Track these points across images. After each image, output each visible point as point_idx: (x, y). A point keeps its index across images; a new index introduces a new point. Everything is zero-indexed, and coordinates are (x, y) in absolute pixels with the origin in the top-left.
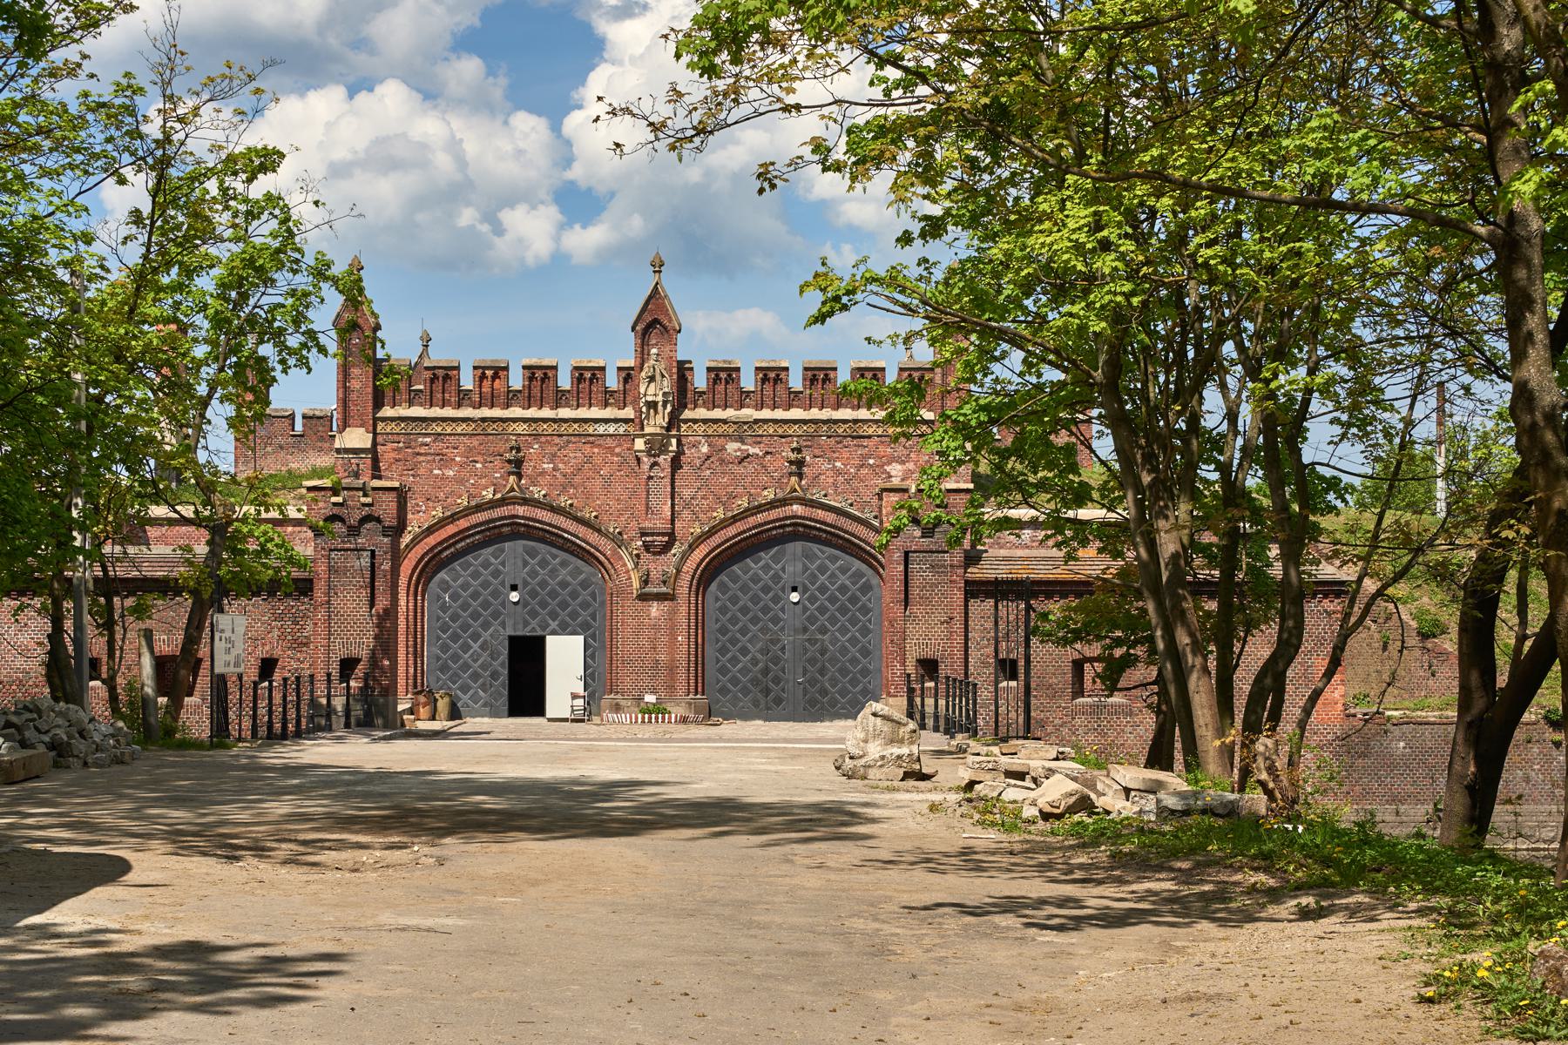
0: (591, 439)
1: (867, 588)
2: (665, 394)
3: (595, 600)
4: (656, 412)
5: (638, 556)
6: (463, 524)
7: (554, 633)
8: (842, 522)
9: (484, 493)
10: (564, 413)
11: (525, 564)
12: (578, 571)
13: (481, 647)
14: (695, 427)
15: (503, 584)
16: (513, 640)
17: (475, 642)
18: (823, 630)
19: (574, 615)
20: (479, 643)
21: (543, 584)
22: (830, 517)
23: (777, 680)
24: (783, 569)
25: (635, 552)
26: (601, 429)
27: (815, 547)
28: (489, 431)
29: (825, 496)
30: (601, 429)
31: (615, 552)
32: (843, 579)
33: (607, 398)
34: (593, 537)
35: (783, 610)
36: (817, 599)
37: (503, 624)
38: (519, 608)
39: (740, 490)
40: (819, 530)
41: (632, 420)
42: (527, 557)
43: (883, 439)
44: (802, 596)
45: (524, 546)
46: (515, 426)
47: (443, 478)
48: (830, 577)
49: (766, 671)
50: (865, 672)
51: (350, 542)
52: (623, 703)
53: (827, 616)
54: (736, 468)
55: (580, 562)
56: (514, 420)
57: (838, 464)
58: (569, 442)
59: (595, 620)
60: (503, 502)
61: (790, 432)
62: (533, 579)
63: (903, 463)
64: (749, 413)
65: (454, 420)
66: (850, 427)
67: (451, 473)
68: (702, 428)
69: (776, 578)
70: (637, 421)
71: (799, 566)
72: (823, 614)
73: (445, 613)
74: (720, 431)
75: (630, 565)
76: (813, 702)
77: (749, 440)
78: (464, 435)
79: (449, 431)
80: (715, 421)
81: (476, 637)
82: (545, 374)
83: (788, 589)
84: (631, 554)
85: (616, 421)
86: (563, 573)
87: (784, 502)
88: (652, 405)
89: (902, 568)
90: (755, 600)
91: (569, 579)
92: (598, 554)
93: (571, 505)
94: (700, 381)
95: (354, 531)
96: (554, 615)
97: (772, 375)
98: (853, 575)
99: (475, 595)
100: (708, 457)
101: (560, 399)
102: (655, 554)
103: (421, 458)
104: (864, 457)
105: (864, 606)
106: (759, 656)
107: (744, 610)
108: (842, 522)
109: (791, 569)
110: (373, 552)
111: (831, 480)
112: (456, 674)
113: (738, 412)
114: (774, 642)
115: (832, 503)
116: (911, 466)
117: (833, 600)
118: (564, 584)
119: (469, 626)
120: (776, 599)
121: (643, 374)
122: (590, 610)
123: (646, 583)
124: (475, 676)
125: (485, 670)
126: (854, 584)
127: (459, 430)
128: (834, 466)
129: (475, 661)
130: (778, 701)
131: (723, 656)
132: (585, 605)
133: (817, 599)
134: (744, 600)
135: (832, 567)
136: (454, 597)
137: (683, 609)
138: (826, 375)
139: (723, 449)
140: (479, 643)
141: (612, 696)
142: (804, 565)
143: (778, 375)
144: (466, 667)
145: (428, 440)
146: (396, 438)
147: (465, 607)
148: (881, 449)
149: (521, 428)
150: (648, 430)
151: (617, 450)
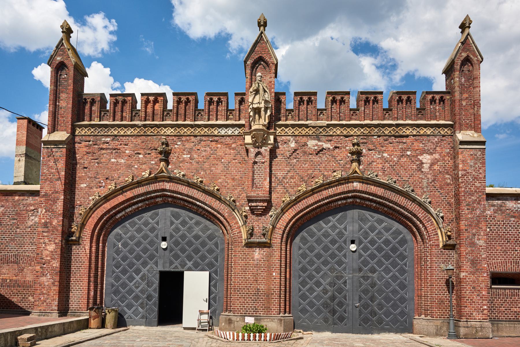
0: (216, 138)
1: (403, 242)
7: (189, 269)
8: (389, 194)
9: (143, 173)
12: (207, 228)
13: (141, 278)
14: (286, 130)
15: (157, 236)
16: (163, 275)
17: (137, 275)
19: (203, 258)
20: (140, 276)
21: (183, 237)
22: (380, 191)
23: (340, 304)
28: (148, 133)
29: (377, 176)
30: (223, 132)
31: (230, 215)
32: (387, 235)
34: (216, 204)
35: (345, 256)
38: (167, 252)
43: (417, 138)
45: (172, 212)
48: (377, 234)
49: (333, 298)
50: (403, 300)
52: (234, 318)
53: (375, 260)
54: (316, 159)
55: (208, 223)
57: (385, 155)
59: (217, 261)
60: (155, 179)
61: (352, 133)
63: (431, 154)
67: (123, 161)
69: (341, 234)
71: (356, 226)
72: (372, 259)
73: (118, 255)
74: (304, 133)
75: (241, 223)
76: (366, 320)
77: (324, 139)
81: (137, 272)
83: (349, 242)
86: (197, 230)
87: (346, 180)
88: (257, 111)
91: (200, 233)
92: (219, 216)
99: (138, 244)
102: (257, 215)
105: (401, 254)
106: (328, 287)
107: (318, 256)
108: (389, 194)
109: (351, 228)
111: (381, 166)
112: (124, 296)
114: (339, 278)
116: (437, 156)
119: (134, 264)
122: (214, 255)
123: (251, 235)
125: (144, 294)
128: (383, 157)
130: (341, 319)
131: (304, 287)
132: (210, 251)
134: (318, 249)
135: (379, 227)
136: (125, 245)
137: (277, 254)
139: (305, 145)
140: (140, 276)
141: (227, 313)
142: (360, 225)
144: (130, 292)
145: (108, 139)
147: (131, 251)
148: (416, 144)
149: (169, 131)
151: (233, 146)
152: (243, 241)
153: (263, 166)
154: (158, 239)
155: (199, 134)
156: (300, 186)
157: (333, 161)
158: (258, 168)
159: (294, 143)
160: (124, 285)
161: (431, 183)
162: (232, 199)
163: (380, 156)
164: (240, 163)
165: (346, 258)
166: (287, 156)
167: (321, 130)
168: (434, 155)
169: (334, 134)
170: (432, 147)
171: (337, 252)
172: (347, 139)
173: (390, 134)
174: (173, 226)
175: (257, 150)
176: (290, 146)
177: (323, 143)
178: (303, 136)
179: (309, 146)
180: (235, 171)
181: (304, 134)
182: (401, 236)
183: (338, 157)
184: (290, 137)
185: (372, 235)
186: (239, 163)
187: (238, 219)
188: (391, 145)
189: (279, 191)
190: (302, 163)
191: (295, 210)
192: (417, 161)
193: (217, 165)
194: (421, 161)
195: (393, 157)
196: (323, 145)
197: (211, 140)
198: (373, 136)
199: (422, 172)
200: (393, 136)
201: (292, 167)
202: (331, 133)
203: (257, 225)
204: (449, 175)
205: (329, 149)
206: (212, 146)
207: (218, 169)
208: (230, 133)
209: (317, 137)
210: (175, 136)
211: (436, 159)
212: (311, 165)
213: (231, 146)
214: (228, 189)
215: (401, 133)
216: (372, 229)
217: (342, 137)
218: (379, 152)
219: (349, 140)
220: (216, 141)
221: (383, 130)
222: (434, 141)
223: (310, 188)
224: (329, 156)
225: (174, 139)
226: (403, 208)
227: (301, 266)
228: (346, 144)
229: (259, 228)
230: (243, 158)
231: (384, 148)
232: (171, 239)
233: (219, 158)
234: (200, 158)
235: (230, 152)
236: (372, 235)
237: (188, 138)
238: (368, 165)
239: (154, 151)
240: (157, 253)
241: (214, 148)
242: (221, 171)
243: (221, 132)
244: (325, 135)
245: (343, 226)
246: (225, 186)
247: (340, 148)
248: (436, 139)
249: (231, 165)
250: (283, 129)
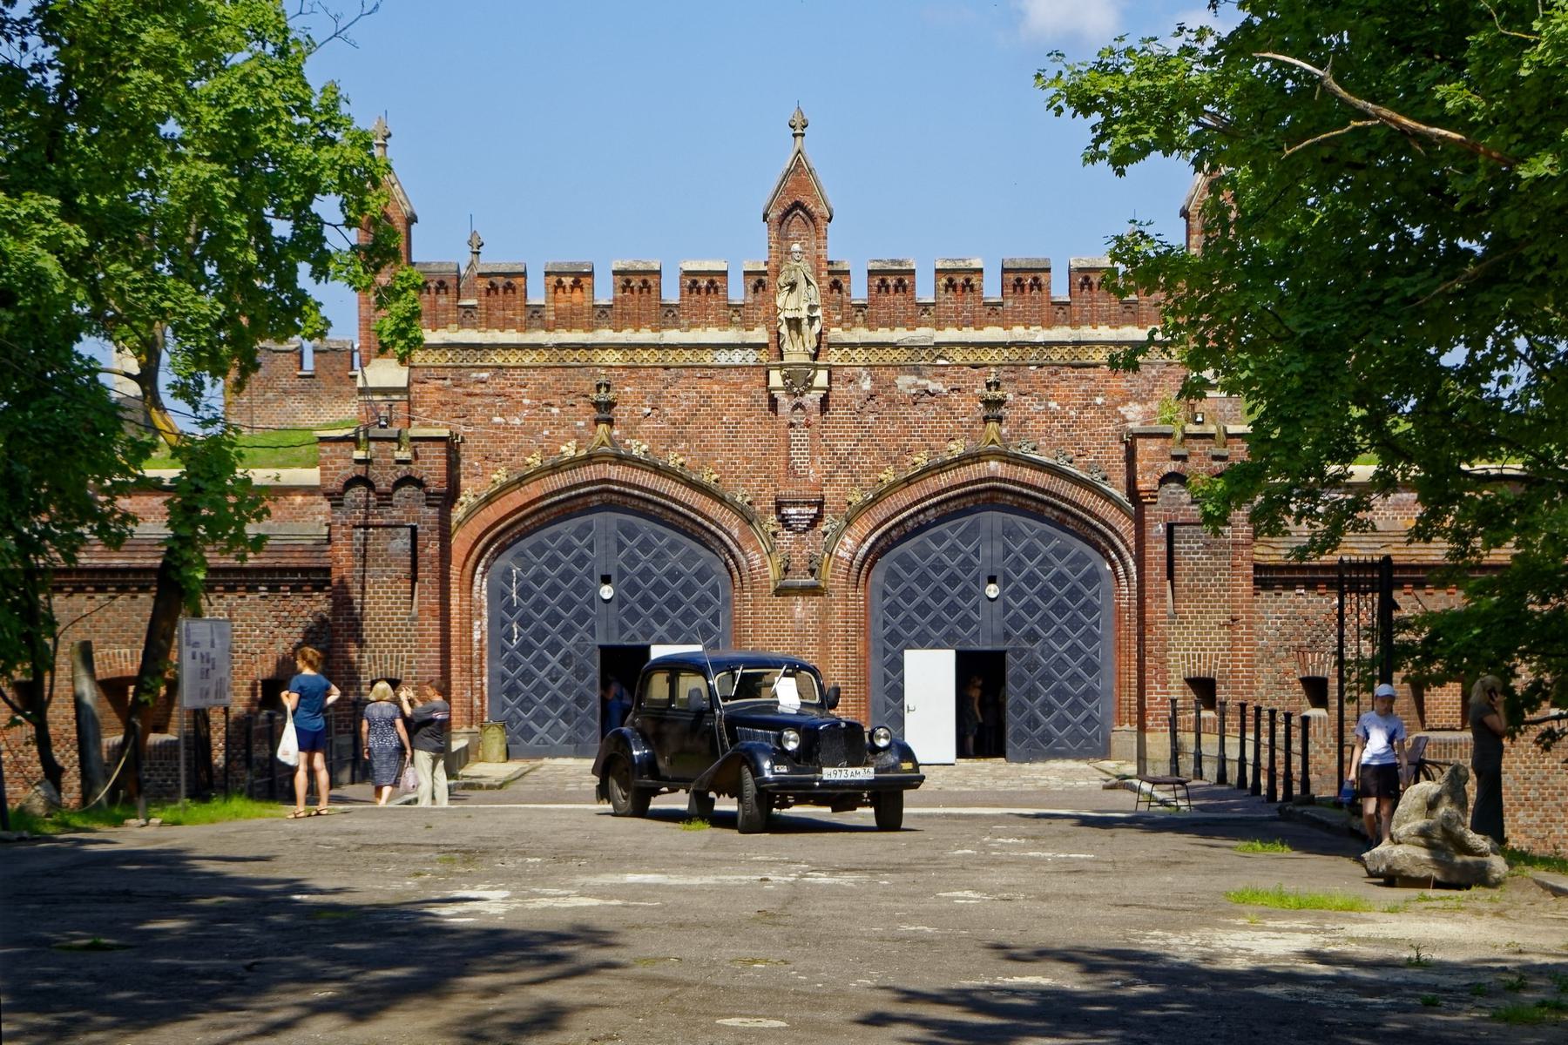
0: (709, 372)
2: (812, 308)
3: (717, 597)
4: (799, 332)
5: (774, 534)
6: (533, 490)
10: (672, 336)
11: (621, 546)
12: (690, 558)
13: (563, 661)
14: (853, 354)
15: (590, 574)
16: (607, 652)
17: (554, 654)
18: (1032, 636)
19: (688, 617)
20: (559, 656)
21: (646, 574)
22: (1041, 479)
24: (976, 553)
25: (772, 529)
26: (723, 358)
27: (1020, 521)
28: (569, 362)
30: (723, 358)
32: (1060, 566)
33: (737, 315)
34: (714, 510)
35: (976, 608)
36: (1023, 594)
37: (591, 630)
38: (613, 607)
39: (916, 442)
40: (1027, 496)
41: (766, 346)
42: (623, 538)
44: (1002, 590)
45: (619, 522)
46: (603, 354)
47: (507, 427)
48: (1041, 563)
50: (1090, 694)
51: (380, 514)
53: (1038, 616)
55: (694, 545)
56: (603, 347)
58: (679, 376)
59: (717, 624)
60: (589, 459)
61: (986, 360)
62: (632, 567)
63: (1144, 401)
64: (924, 334)
65: (520, 347)
66: (1070, 353)
67: (517, 421)
68: (860, 356)
69: (967, 564)
70: (773, 346)
71: (999, 549)
77: (929, 372)
78: (535, 368)
79: (513, 362)
80: (881, 345)
81: (554, 647)
82: (645, 282)
85: (743, 346)
86: (673, 560)
89: (1163, 548)
90: (938, 594)
91: (681, 567)
92: (720, 533)
93: (682, 465)
94: (859, 290)
95: (385, 499)
96: (660, 617)
97: (960, 280)
98: (1072, 561)
99: (553, 590)
101: (668, 315)
103: (476, 401)
104: (1090, 394)
107: (923, 609)
109: (988, 552)
110: (414, 529)
112: (528, 699)
113: (911, 333)
115: (1044, 459)
117: (1045, 594)
118: (673, 575)
119: (545, 633)
120: (966, 594)
121: (781, 280)
122: (711, 611)
123: (786, 570)
124: (554, 701)
125: (569, 694)
126: (1075, 572)
127: (527, 361)
128: (1048, 408)
129: (554, 680)
133: (1023, 594)
135: (1045, 549)
137: (839, 608)
138: (1036, 279)
140: (559, 656)
142: (1005, 545)
143: (968, 280)
144: (541, 689)
145: (485, 375)
146: (441, 373)
148: (1113, 382)
149: (613, 357)
150: (787, 359)
152: (772, 584)
154: (592, 579)
155: (674, 363)
156: (881, 470)
160: (527, 676)
163: (1042, 407)
165: (978, 613)
167: (923, 353)
168: (1150, 404)
170: (1146, 387)
171: (960, 602)
172: (976, 371)
173: (1062, 362)
174: (623, 554)
177: (929, 382)
178: (888, 366)
182: (1088, 566)
185: (1031, 565)
188: (1064, 383)
192: (1115, 417)
194: (1123, 416)
198: (1029, 365)
209: (917, 371)
210: (623, 367)
215: (1084, 360)
216: (1031, 552)
218: (1040, 400)
221: (1048, 352)
223: (903, 476)
226: (1088, 512)
227: (888, 629)
231: (1049, 392)
232: (620, 580)
236: (1031, 565)
238: (1019, 426)
239: (582, 399)
240: (593, 609)
245: (971, 548)
248: (1154, 372)
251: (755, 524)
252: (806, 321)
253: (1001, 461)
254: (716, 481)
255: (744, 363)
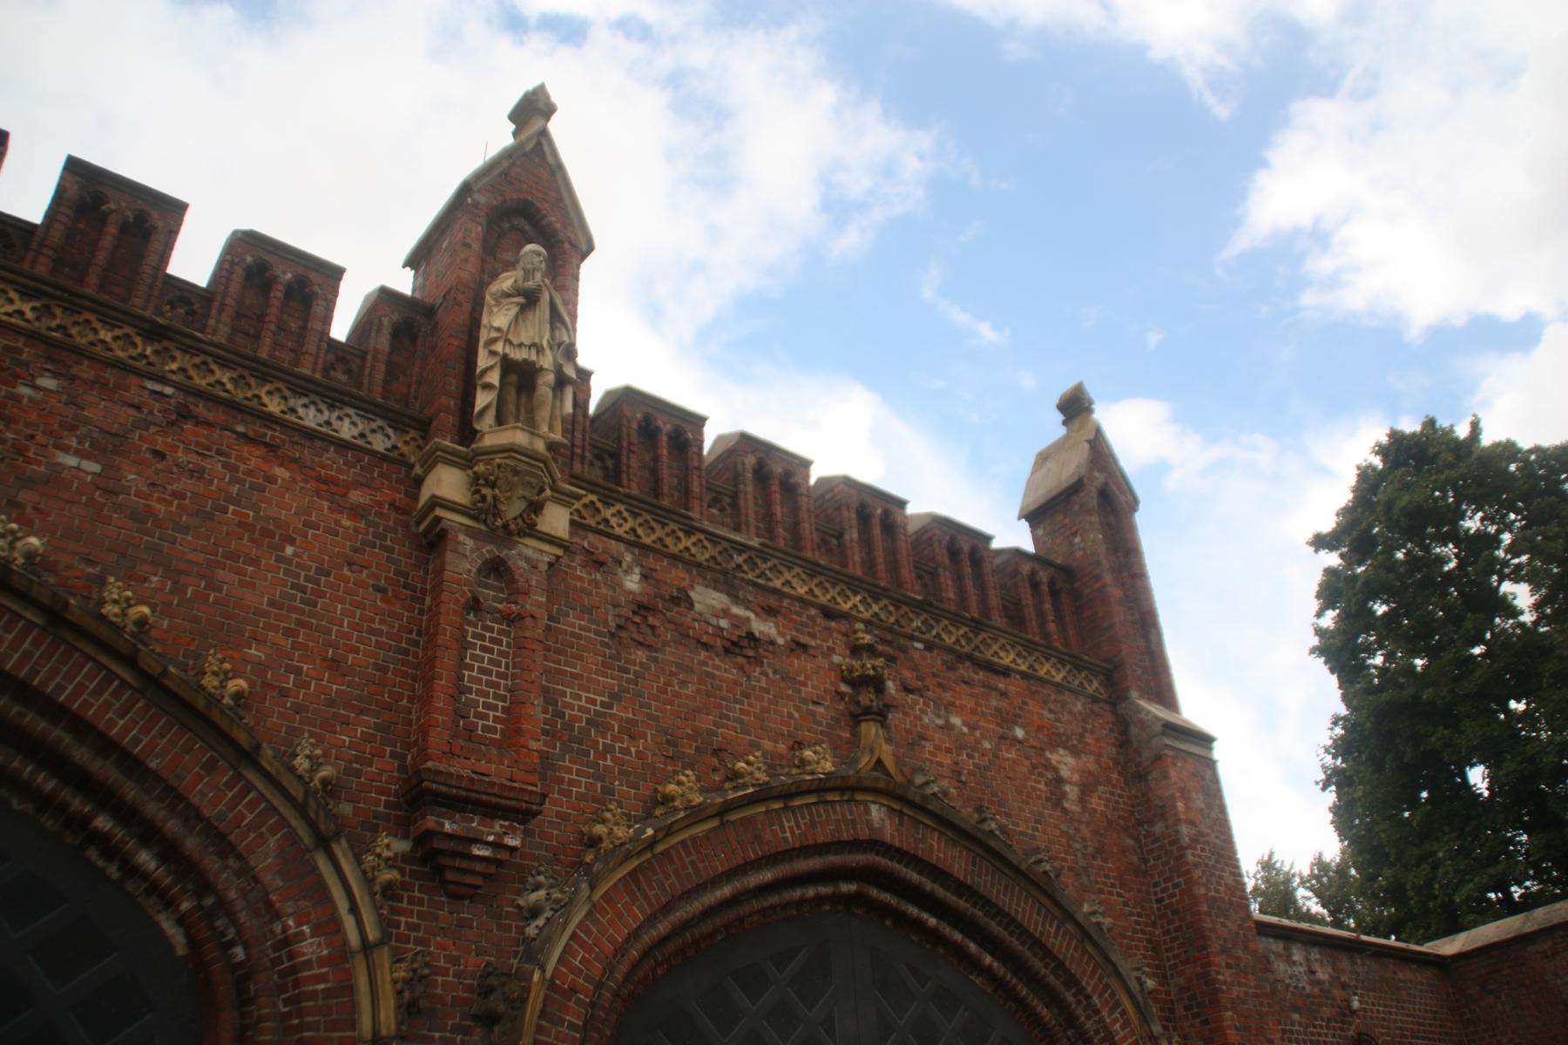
5: (388, 888)
25: (388, 875)
54: (725, 670)
58: (184, 414)
61: (846, 606)
84: (368, 880)
93: (142, 622)
100: (642, 608)
108: (988, 882)
139: (682, 600)
151: (356, 496)
153: (507, 634)
157: (790, 698)
158: (483, 638)
159: (636, 577)
161: (1094, 858)
162: (325, 772)
163: (940, 722)
164: (383, 590)
166: (606, 624)
169: (786, 589)
175: (489, 550)
176: (621, 585)
177: (752, 616)
179: (698, 607)
180: (352, 626)
181: (674, 550)
183: (805, 685)
184: (622, 547)
186: (377, 589)
187: (343, 905)
189: (572, 783)
190: (672, 674)
191: (646, 897)
193: (254, 562)
194: (1056, 770)
195: (978, 733)
196: (748, 619)
197: (240, 429)
198: (913, 638)
199: (1065, 811)
200: (970, 657)
201: (629, 681)
202: (777, 583)
203: (449, 959)
204: (1131, 836)
205: (772, 643)
206: (241, 459)
207: (252, 586)
208: (346, 431)
211: (1090, 773)
212: (708, 694)
213: (345, 495)
214: (298, 709)
217: (813, 612)
218: (937, 705)
219: (840, 632)
220: (267, 445)
222: (1076, 710)
224: (775, 672)
225: (20, 352)
228: (830, 644)
229: (457, 975)
230: (397, 573)
231: (948, 696)
233: (270, 534)
234: (161, 500)
235: (337, 522)
237: (110, 375)
241: (250, 473)
242: (272, 603)
243: (301, 411)
244: (754, 584)
246: (284, 693)
247: (811, 652)
249: (330, 585)
250: (592, 502)
251: (341, 850)
252: (551, 378)
253: (891, 809)
254: (238, 696)
255: (359, 442)
